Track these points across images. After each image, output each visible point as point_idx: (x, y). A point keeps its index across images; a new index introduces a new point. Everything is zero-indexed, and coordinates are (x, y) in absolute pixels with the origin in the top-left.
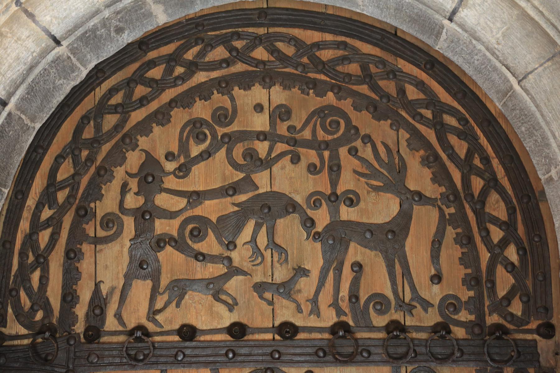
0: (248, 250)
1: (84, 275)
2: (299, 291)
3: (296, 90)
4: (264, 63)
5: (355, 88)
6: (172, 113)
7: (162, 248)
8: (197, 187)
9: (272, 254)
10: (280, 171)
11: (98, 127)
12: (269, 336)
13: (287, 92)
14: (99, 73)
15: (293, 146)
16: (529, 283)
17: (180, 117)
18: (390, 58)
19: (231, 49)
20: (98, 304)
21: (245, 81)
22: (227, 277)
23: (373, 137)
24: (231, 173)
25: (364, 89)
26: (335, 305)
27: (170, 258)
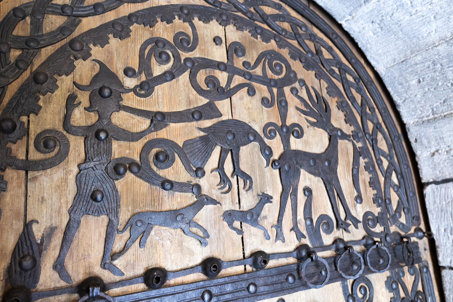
0: (215, 177)
2: (265, 217)
3: (246, 33)
5: (289, 40)
6: (131, 28)
7: (121, 175)
8: (161, 108)
10: (239, 101)
12: (240, 269)
13: (240, 33)
15: (249, 80)
17: (140, 34)
23: (307, 82)
24: (195, 97)
25: (295, 43)
27: (130, 186)
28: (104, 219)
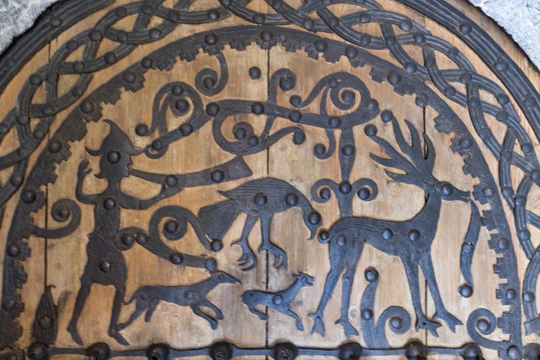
0: (237, 250)
1: (31, 276)
2: (300, 303)
3: (302, 53)
4: (263, 16)
5: (374, 52)
6: (146, 75)
7: (128, 246)
8: (175, 168)
9: (267, 256)
10: (280, 152)
13: (291, 54)
15: (296, 122)
17: (155, 80)
18: (416, 18)
21: (239, 39)
22: (210, 284)
23: (395, 115)
24: (218, 153)
25: (385, 54)
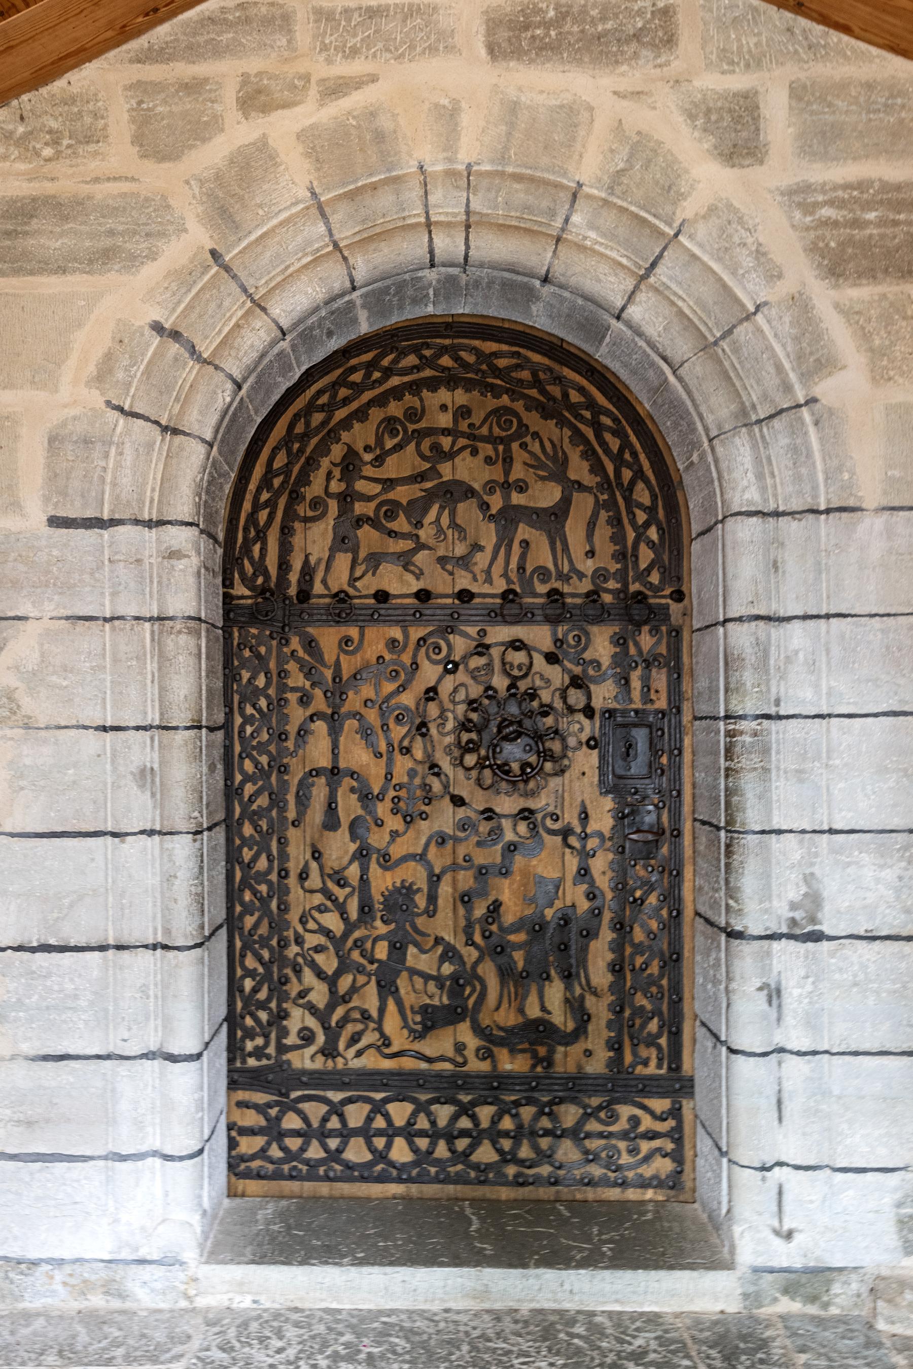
1: (296, 548)
3: (476, 393)
4: (449, 369)
11: (307, 424)
12: (449, 601)
14: (309, 377)
16: (666, 557)
17: (377, 415)
18: (556, 367)
19: (421, 357)
20: (307, 572)
21: (433, 385)
22: (415, 551)
25: (534, 393)
26: (505, 575)
27: (367, 536)
28: (350, 556)
